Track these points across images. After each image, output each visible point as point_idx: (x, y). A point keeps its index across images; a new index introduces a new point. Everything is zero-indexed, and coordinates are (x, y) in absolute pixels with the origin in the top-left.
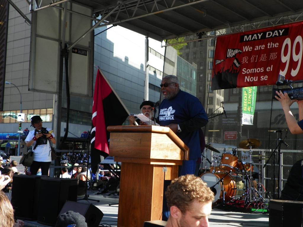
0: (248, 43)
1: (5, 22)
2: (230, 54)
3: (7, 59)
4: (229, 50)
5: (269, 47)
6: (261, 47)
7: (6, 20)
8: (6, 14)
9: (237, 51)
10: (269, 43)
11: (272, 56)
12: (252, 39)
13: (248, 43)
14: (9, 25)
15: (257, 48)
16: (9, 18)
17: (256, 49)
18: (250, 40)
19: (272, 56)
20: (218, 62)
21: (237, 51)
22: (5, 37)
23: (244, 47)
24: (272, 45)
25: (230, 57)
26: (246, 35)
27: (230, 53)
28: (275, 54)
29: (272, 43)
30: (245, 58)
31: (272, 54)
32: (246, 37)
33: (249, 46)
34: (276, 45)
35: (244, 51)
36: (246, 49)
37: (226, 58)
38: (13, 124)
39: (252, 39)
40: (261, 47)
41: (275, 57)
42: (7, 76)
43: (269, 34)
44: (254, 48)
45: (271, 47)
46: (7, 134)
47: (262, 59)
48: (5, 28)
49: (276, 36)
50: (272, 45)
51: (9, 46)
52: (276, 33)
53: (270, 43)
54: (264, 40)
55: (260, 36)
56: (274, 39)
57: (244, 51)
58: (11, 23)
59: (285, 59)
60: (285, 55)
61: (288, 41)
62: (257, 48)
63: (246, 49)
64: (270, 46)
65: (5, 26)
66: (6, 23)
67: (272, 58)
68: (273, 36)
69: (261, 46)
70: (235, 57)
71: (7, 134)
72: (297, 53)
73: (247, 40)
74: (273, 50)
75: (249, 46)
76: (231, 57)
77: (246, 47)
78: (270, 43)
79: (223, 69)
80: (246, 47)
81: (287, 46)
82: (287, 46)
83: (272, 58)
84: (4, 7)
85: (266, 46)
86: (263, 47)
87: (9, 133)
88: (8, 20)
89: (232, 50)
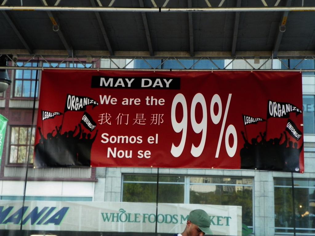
0: (108, 91)
2: (73, 105)
4: (69, 96)
5: (148, 104)
6: (133, 102)
9: (86, 101)
10: (148, 97)
11: (155, 119)
12: (116, 86)
13: (108, 91)
15: (126, 102)
17: (125, 103)
18: (111, 85)
19: (155, 119)
20: (47, 115)
21: (86, 101)
23: (101, 96)
24: (154, 101)
25: (74, 110)
26: (103, 77)
27: (73, 102)
28: (161, 116)
29: (152, 97)
30: (104, 115)
31: (155, 116)
32: (102, 79)
33: (110, 97)
34: (161, 102)
35: (102, 102)
36: (104, 100)
37: (65, 112)
39: (116, 86)
40: (133, 102)
41: (161, 121)
43: (147, 83)
44: (120, 101)
45: (152, 104)
47: (138, 121)
49: (158, 87)
50: (154, 101)
52: (158, 82)
53: (150, 98)
54: (136, 90)
55: (130, 84)
56: (157, 92)
57: (102, 102)
59: (179, 127)
60: (179, 119)
61: (180, 98)
62: (126, 102)
63: (104, 100)
64: (150, 102)
67: (155, 122)
68: (154, 86)
69: (133, 99)
70: (84, 110)
72: (199, 120)
73: (106, 85)
74: (156, 109)
75: (110, 97)
76: (76, 109)
77: (105, 97)
78: (150, 98)
79: (58, 129)
80: (105, 97)
81: (179, 106)
82: (179, 106)
83: (155, 122)
85: (143, 101)
86: (137, 101)
89: (77, 99)
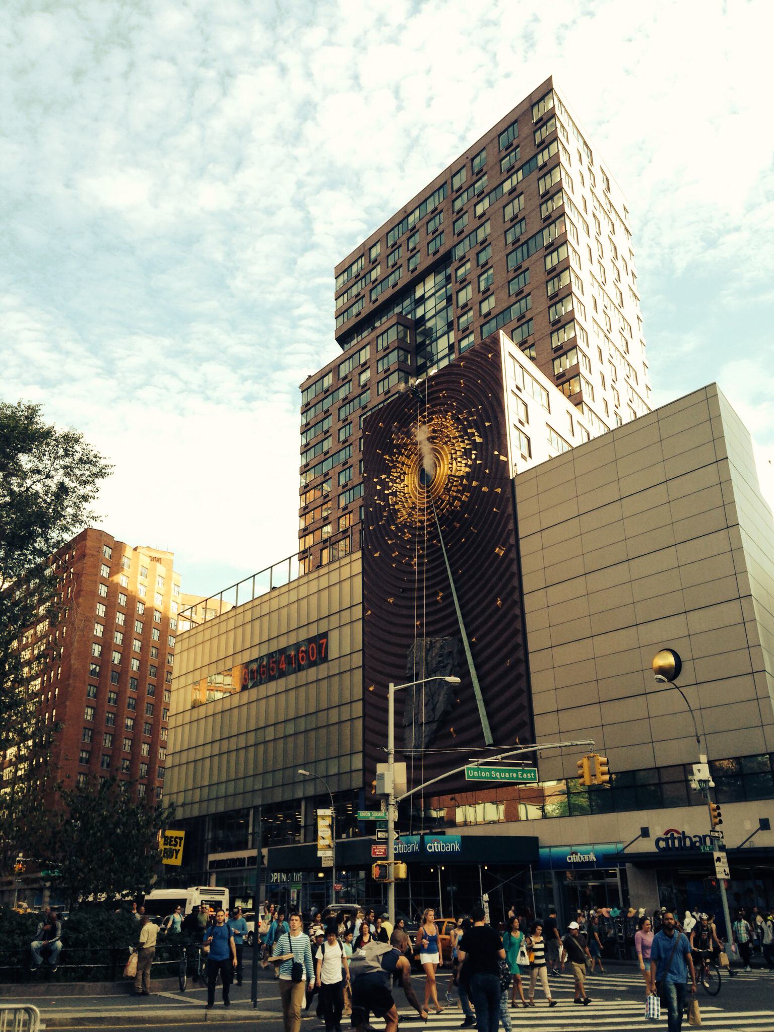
1: (512, 546)
3: (529, 636)
7: (512, 541)
8: (511, 526)
14: (522, 553)
16: (521, 535)
22: (515, 582)
38: (554, 821)
42: (540, 682)
46: (567, 849)
48: (512, 560)
51: (530, 603)
58: (525, 547)
65: (513, 555)
66: (514, 549)
71: (567, 849)
84: (503, 512)
87: (597, 847)
88: (517, 540)
